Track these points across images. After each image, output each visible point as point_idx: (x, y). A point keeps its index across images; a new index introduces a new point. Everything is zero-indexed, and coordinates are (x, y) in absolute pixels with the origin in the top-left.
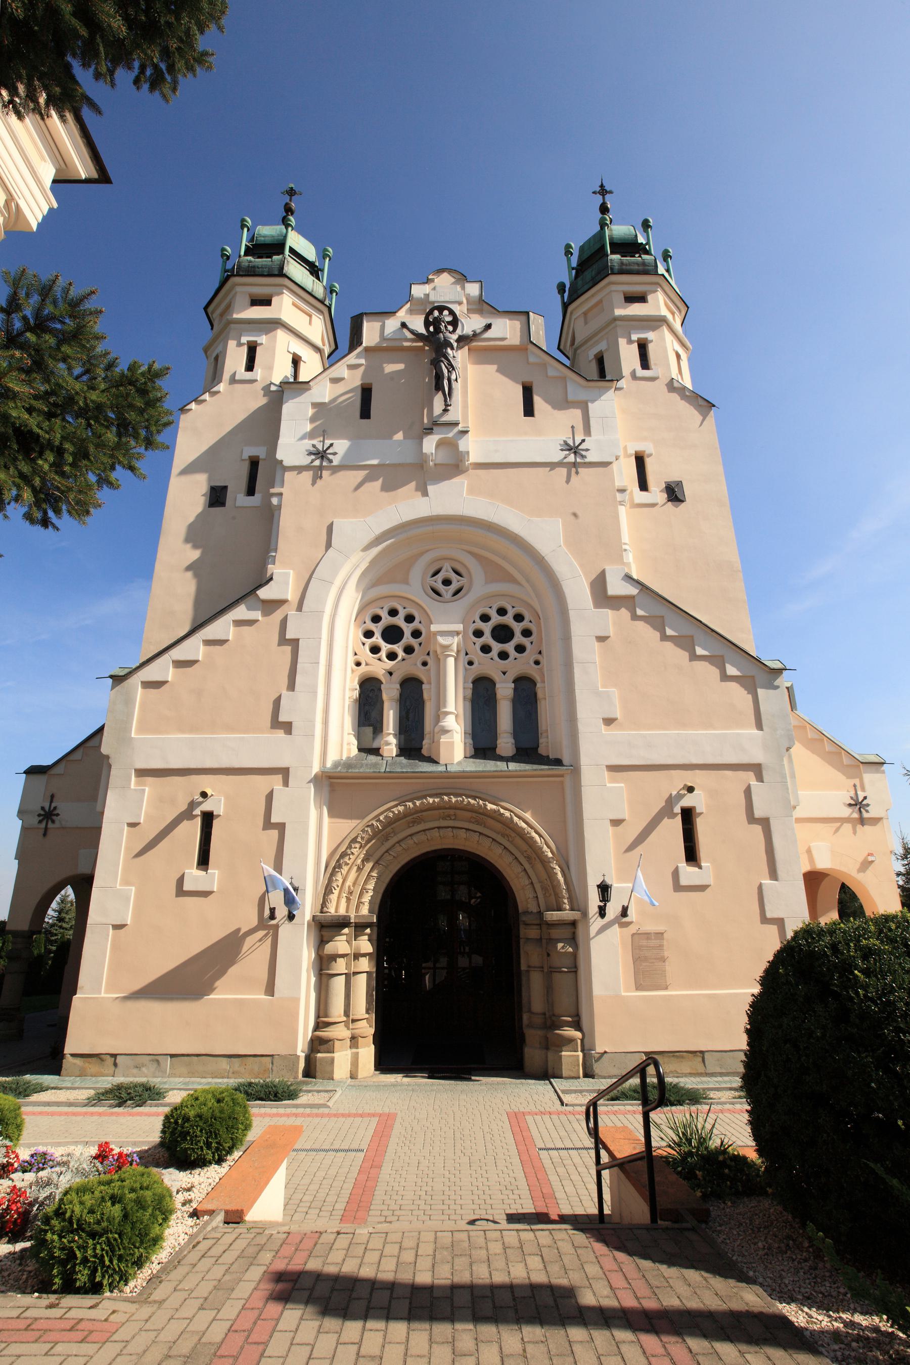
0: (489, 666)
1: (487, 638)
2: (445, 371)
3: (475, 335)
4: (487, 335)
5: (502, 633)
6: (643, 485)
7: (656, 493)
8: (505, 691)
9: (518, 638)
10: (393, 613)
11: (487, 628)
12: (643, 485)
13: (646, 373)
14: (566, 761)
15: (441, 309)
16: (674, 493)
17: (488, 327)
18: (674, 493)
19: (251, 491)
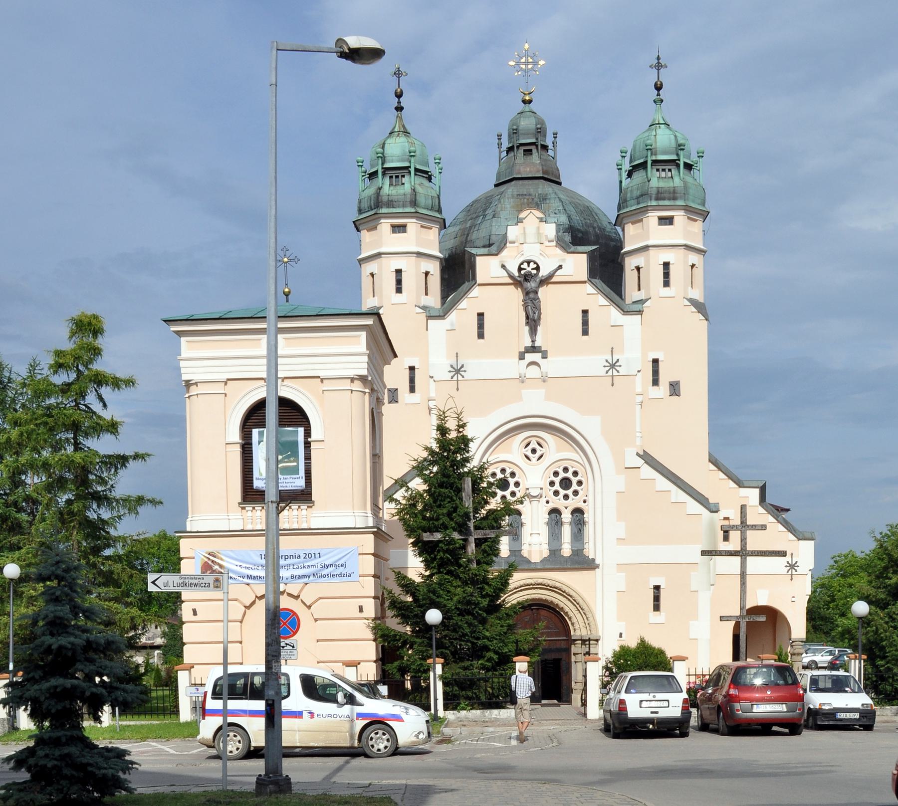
0: (558, 502)
1: (557, 487)
2: (531, 314)
3: (551, 276)
4: (559, 272)
5: (566, 483)
6: (656, 382)
7: (663, 389)
8: (566, 516)
9: (575, 487)
10: (503, 471)
11: (557, 480)
12: (656, 382)
13: (666, 291)
14: (597, 562)
15: (529, 262)
16: (675, 389)
17: (560, 267)
18: (675, 389)
19: (412, 389)
